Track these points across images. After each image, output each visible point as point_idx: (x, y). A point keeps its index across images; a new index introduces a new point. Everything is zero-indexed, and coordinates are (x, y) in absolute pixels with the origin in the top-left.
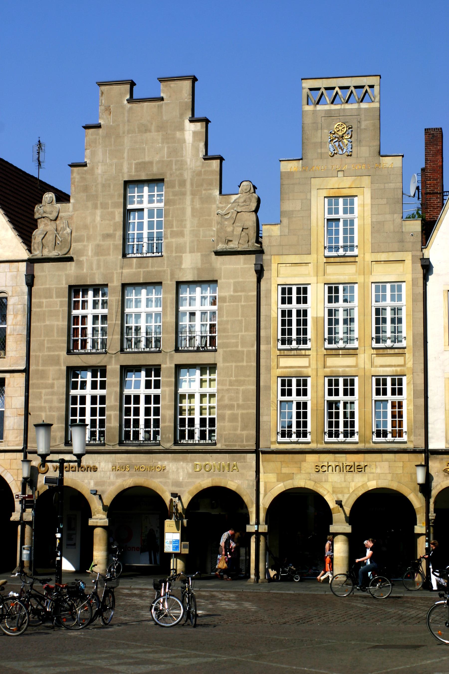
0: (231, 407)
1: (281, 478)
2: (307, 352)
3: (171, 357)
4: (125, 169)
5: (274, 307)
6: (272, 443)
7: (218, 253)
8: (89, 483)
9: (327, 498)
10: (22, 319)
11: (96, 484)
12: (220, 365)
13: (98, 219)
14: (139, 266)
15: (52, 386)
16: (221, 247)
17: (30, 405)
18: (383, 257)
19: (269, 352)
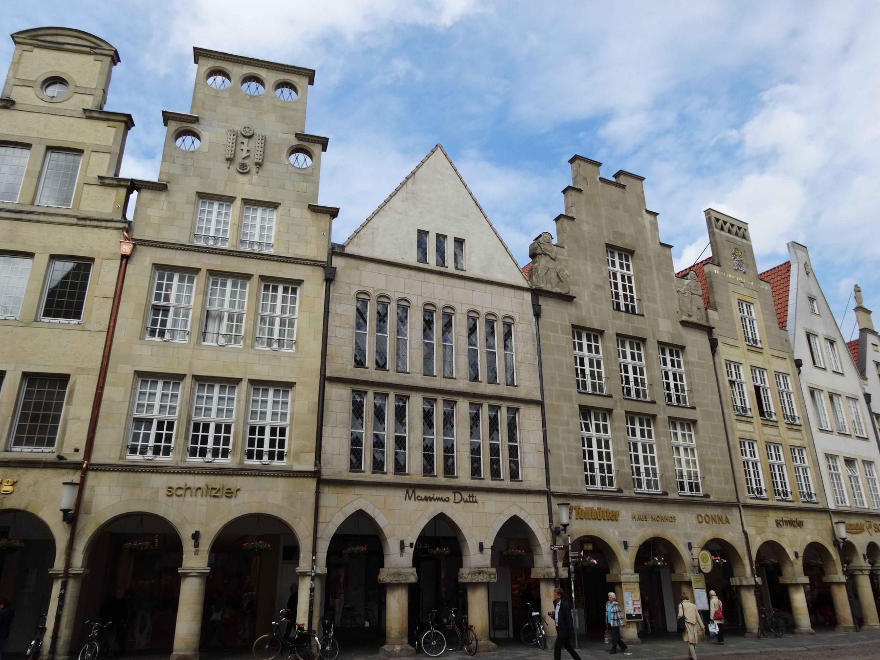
0: (714, 462)
1: (761, 531)
2: (752, 420)
3: (664, 409)
4: (605, 234)
5: (725, 380)
6: (747, 497)
7: (684, 323)
8: (614, 533)
9: (788, 550)
10: (531, 348)
11: (621, 534)
12: (700, 422)
13: (589, 269)
14: (628, 320)
15: (568, 423)
16: (684, 318)
17: (548, 441)
18: (776, 353)
19: (730, 414)
